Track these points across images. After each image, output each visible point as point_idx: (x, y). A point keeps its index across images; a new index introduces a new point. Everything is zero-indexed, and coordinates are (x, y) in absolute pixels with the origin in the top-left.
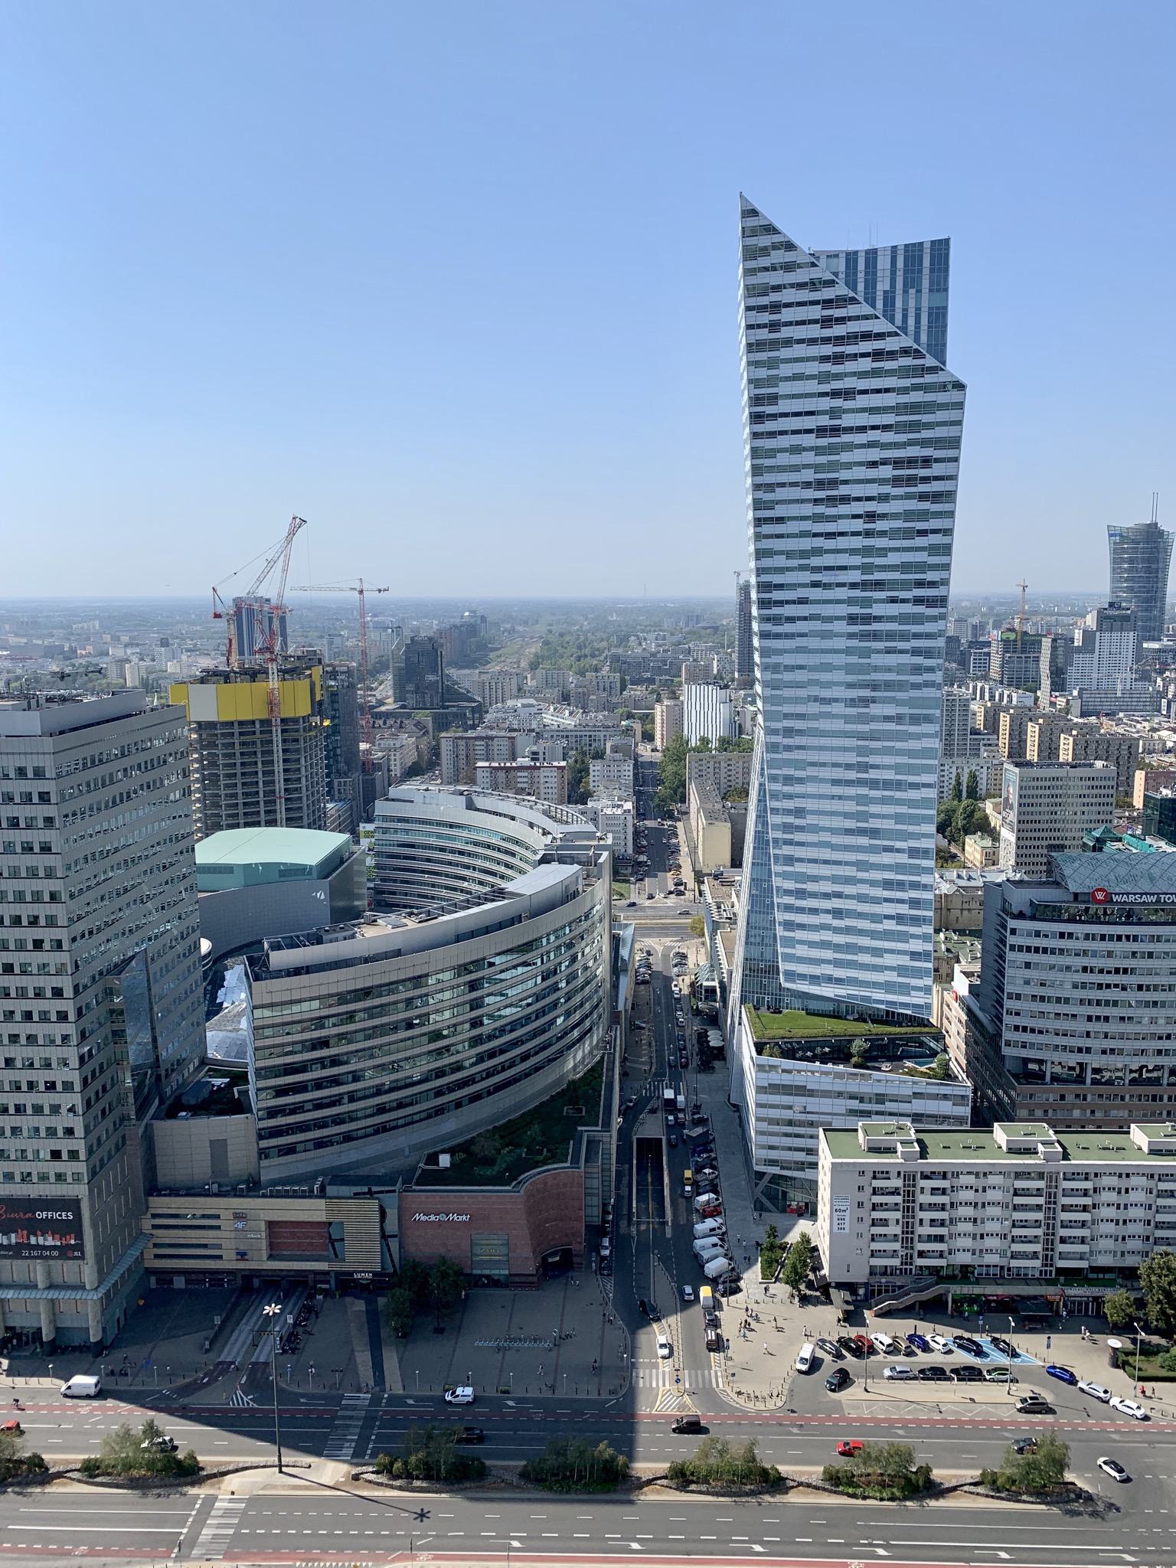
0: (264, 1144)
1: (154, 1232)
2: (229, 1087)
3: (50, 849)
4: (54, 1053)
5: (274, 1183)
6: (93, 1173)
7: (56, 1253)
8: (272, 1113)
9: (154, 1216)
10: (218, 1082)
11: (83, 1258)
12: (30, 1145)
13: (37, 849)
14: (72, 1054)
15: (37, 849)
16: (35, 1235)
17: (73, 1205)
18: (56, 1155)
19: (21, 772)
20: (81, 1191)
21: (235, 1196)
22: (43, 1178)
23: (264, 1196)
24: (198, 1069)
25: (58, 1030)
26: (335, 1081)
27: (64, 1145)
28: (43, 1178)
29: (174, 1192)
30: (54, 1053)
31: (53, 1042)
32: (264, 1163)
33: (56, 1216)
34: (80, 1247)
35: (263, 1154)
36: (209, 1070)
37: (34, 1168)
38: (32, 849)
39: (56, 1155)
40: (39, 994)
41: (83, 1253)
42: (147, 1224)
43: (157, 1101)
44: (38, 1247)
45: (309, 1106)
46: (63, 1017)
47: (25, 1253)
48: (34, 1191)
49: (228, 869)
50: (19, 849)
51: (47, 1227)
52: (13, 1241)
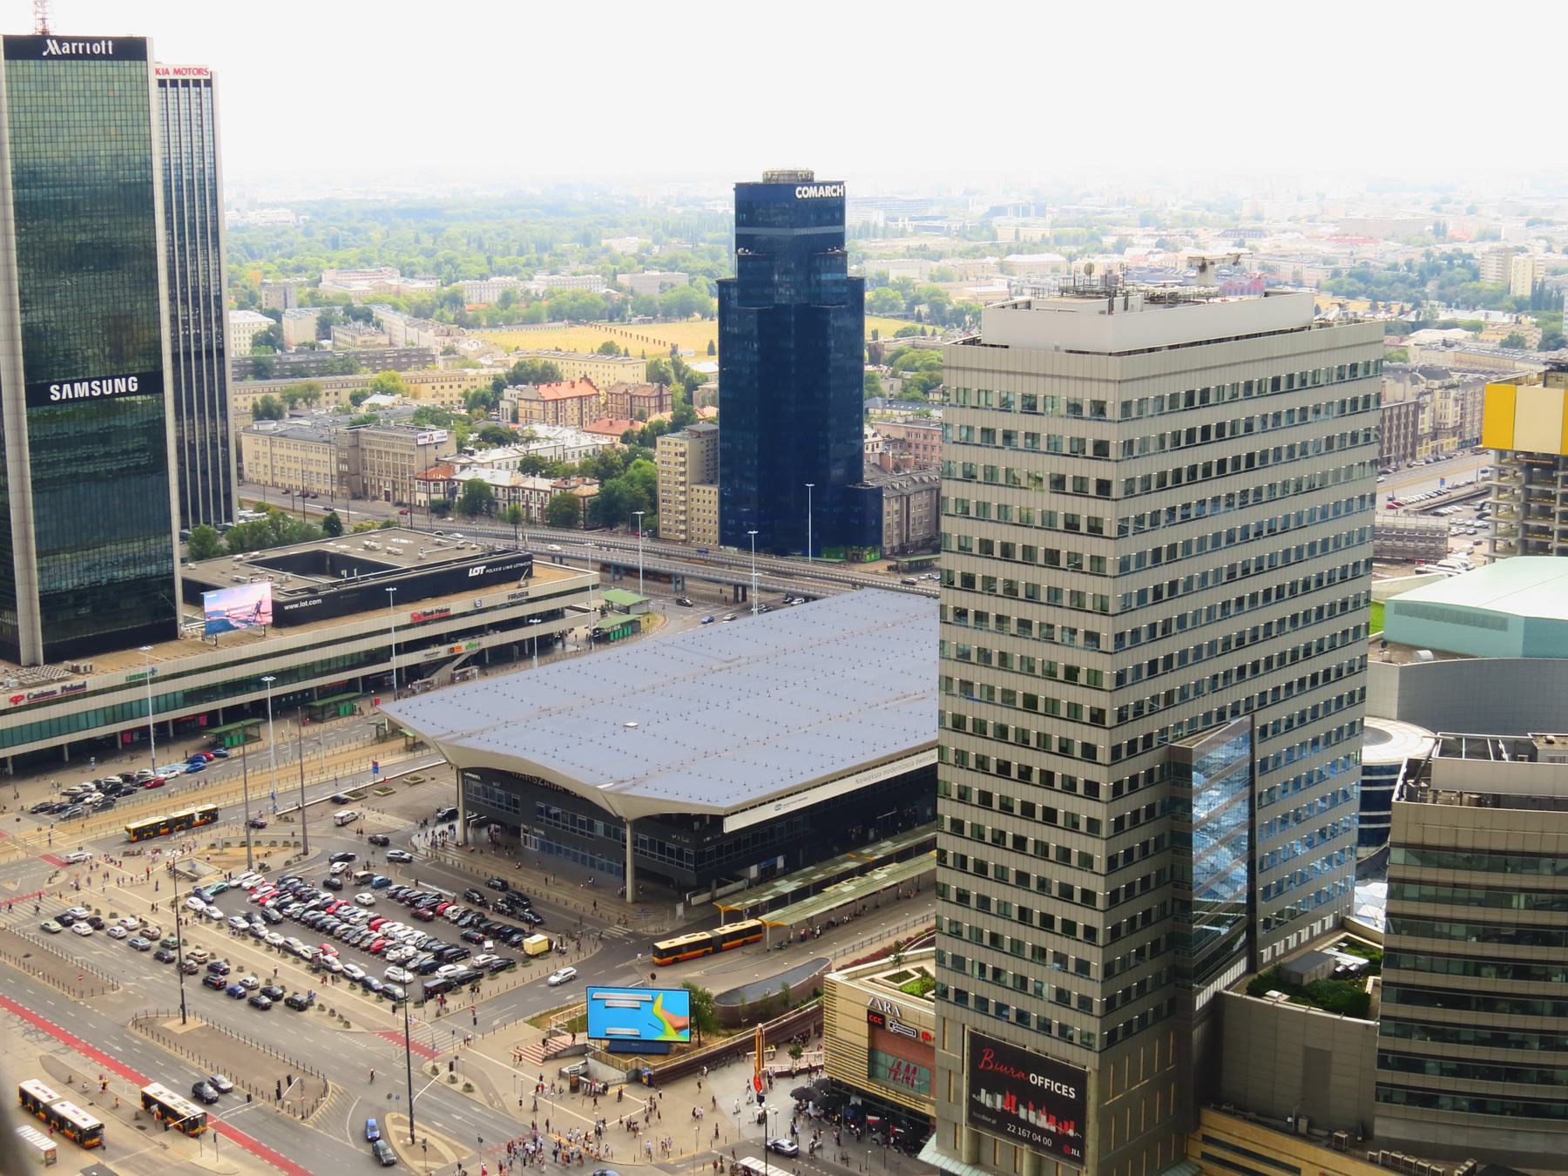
0: (1387, 1076)
1: (1204, 1164)
2: (1363, 972)
3: (1100, 530)
4: (1078, 844)
5: (1393, 1144)
6: (1111, 1039)
7: (1048, 1142)
8: (1403, 1028)
9: (1208, 1140)
10: (1352, 961)
11: (1081, 1161)
12: (1032, 972)
13: (1084, 528)
14: (1098, 850)
15: (1084, 528)
16: (1027, 1107)
17: (1076, 1078)
18: (1062, 997)
19: (1075, 409)
20: (1088, 1061)
21: (1328, 1147)
22: (1045, 1027)
23: (1372, 1161)
24: (1326, 933)
25: (1085, 809)
26: (1523, 1005)
27: (1077, 987)
28: (1045, 1027)
29: (1242, 1110)
30: (1078, 844)
31: (1076, 825)
32: (1382, 1108)
33: (1055, 1086)
34: (1080, 1143)
35: (1386, 1094)
36: (1344, 940)
37: (1036, 1010)
38: (1078, 527)
39: (1062, 997)
40: (1065, 750)
41: (1082, 1153)
42: (1197, 1149)
43: (1241, 967)
44: (1026, 1124)
45: (1467, 1034)
46: (1092, 789)
47: (1011, 1128)
48: (1031, 1041)
49: (1497, 622)
50: (1061, 525)
51: (1042, 1100)
52: (999, 1106)
